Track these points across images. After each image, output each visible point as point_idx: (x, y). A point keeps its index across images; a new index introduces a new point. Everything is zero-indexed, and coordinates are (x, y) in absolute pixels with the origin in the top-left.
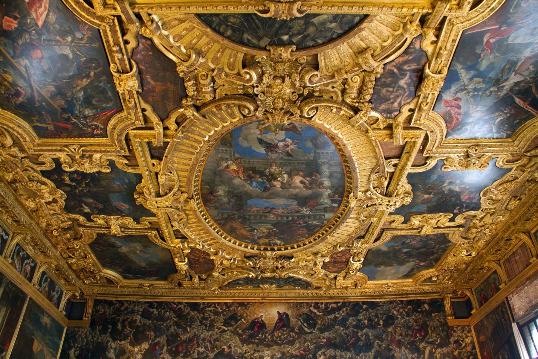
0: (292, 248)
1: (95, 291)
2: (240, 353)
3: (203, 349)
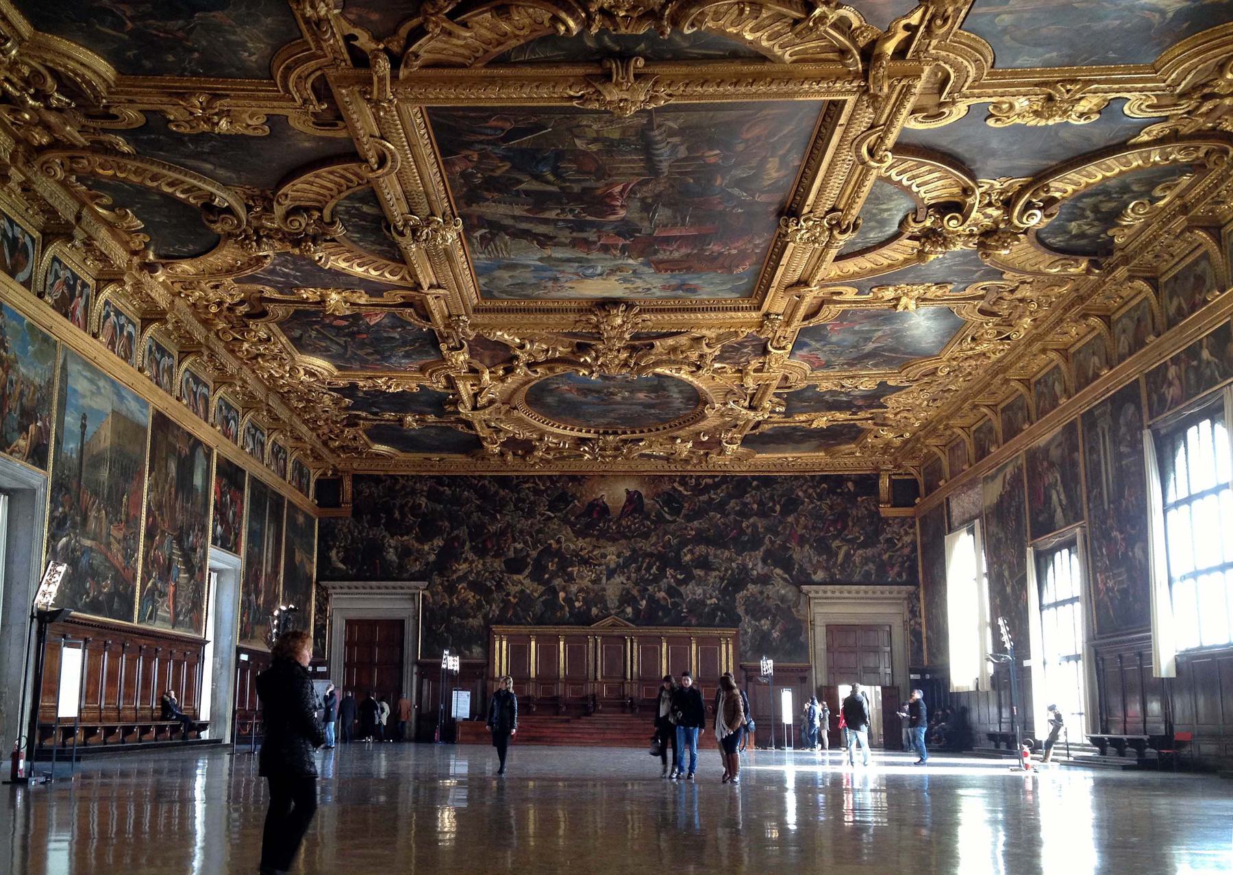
0: (642, 432)
1: (355, 466)
3: (522, 545)
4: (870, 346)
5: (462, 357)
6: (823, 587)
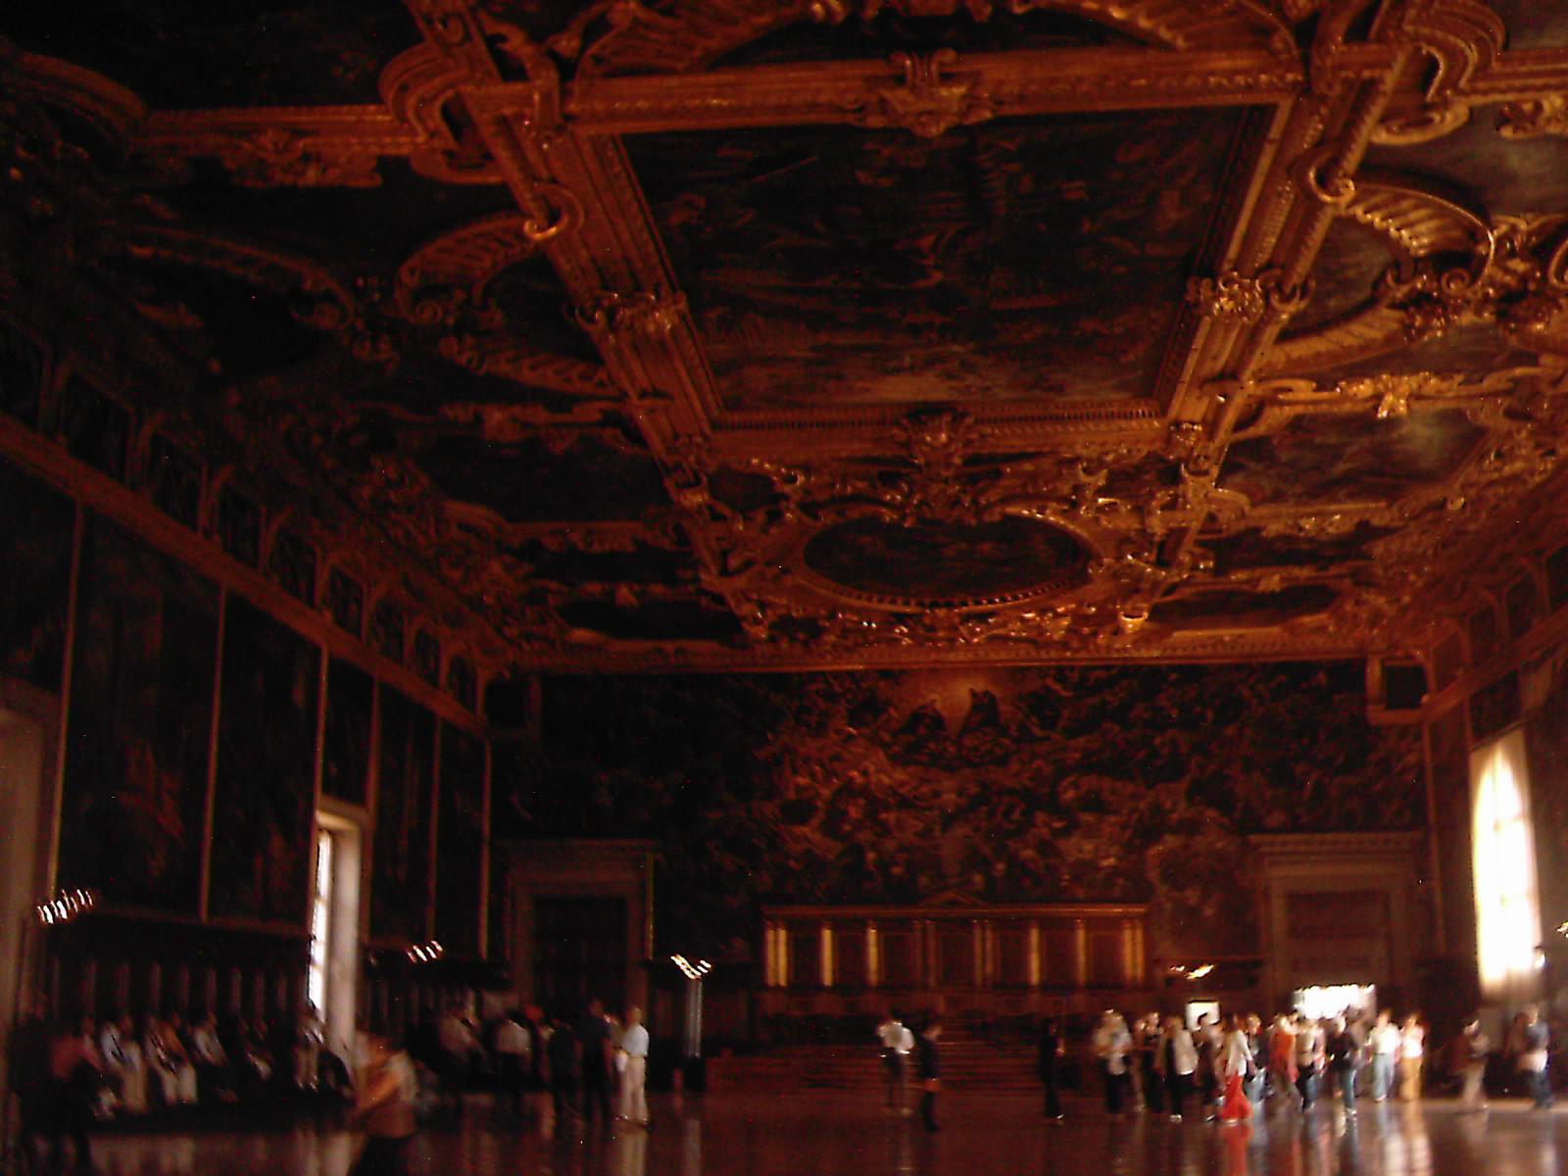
2: (890, 787)
4: (1341, 467)
5: (696, 499)
6: (1281, 837)
